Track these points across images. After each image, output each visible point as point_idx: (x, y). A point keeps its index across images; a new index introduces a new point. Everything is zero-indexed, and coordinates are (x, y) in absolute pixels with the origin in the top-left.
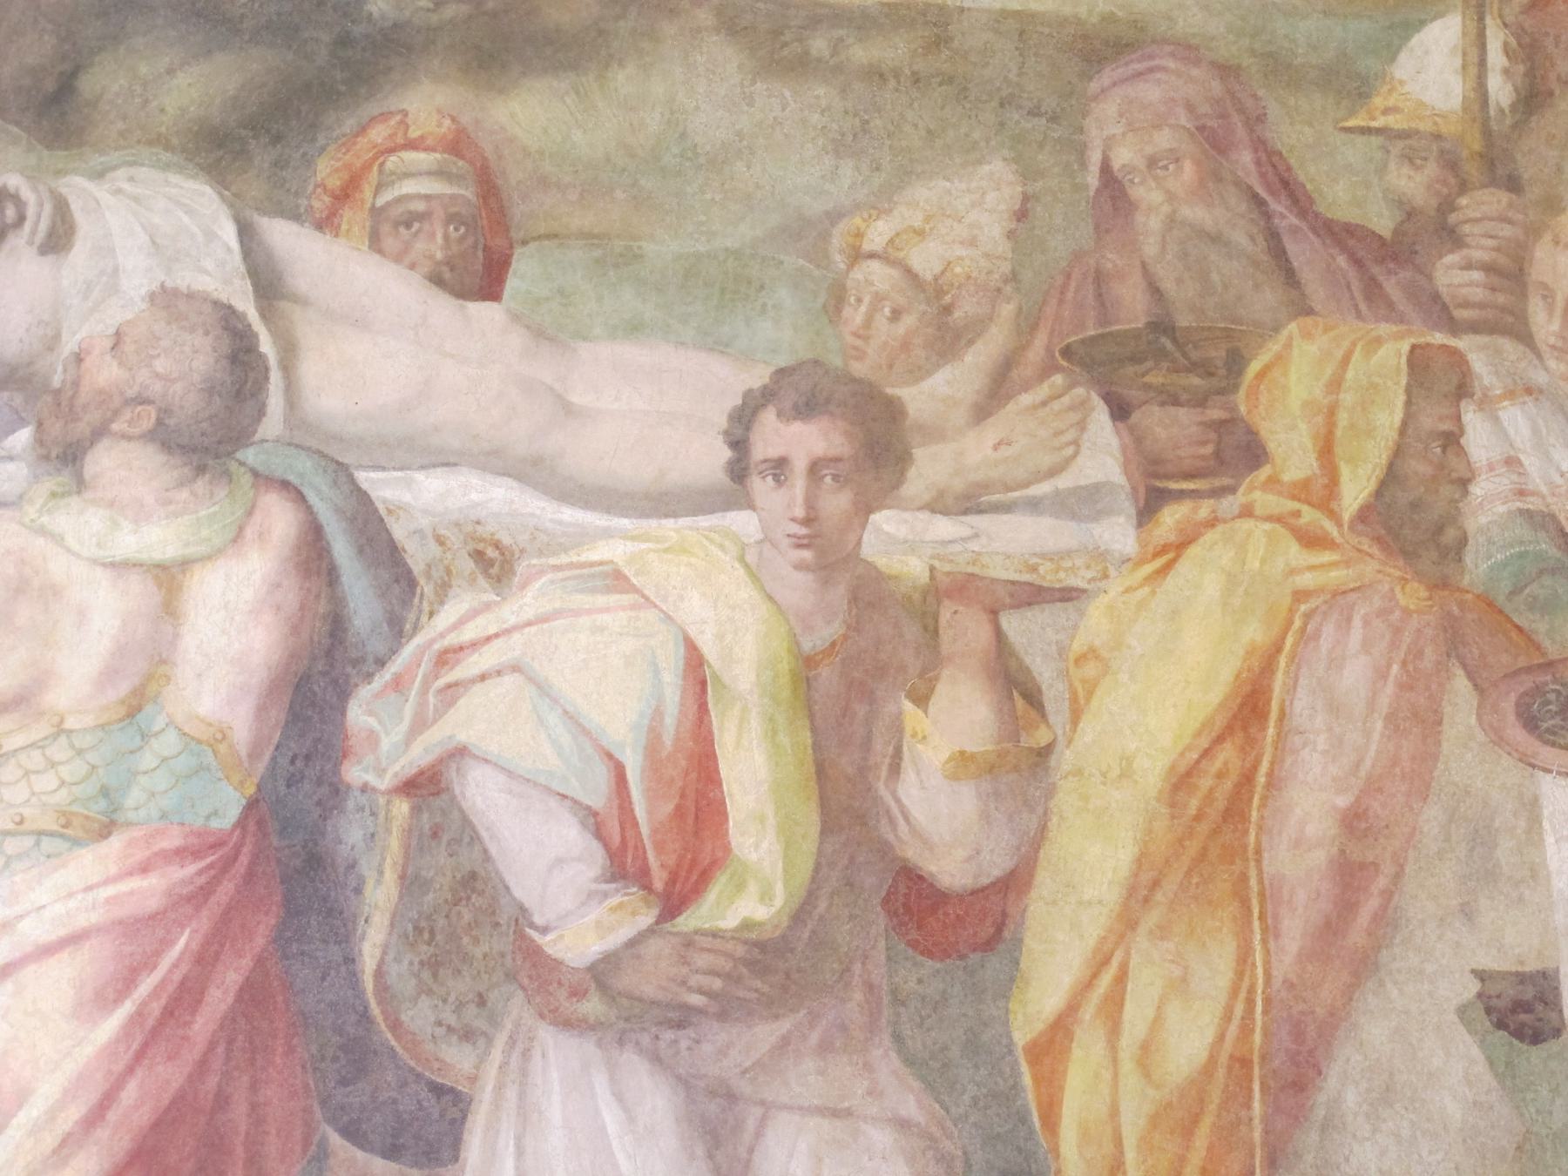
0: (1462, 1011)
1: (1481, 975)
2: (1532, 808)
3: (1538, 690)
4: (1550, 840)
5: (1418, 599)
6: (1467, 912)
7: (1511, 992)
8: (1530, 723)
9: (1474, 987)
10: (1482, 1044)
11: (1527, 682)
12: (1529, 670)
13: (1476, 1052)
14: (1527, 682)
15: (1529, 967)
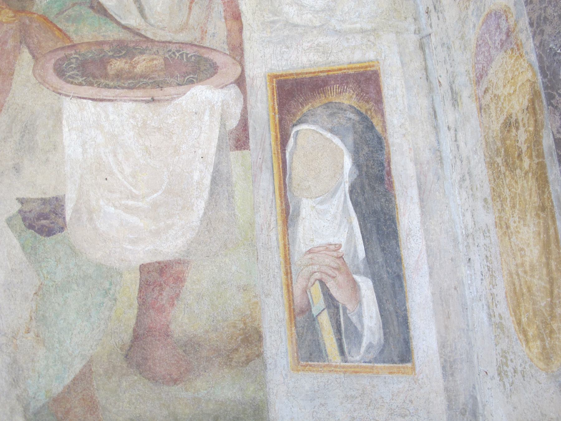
0: (9, 221)
1: (22, 201)
2: (57, 115)
3: (67, 58)
4: (66, 129)
5: (8, 17)
6: (17, 169)
7: (37, 208)
8: (60, 72)
9: (17, 206)
10: (19, 237)
11: (62, 54)
12: (63, 48)
13: (15, 241)
14: (62, 54)
15: (50, 194)
